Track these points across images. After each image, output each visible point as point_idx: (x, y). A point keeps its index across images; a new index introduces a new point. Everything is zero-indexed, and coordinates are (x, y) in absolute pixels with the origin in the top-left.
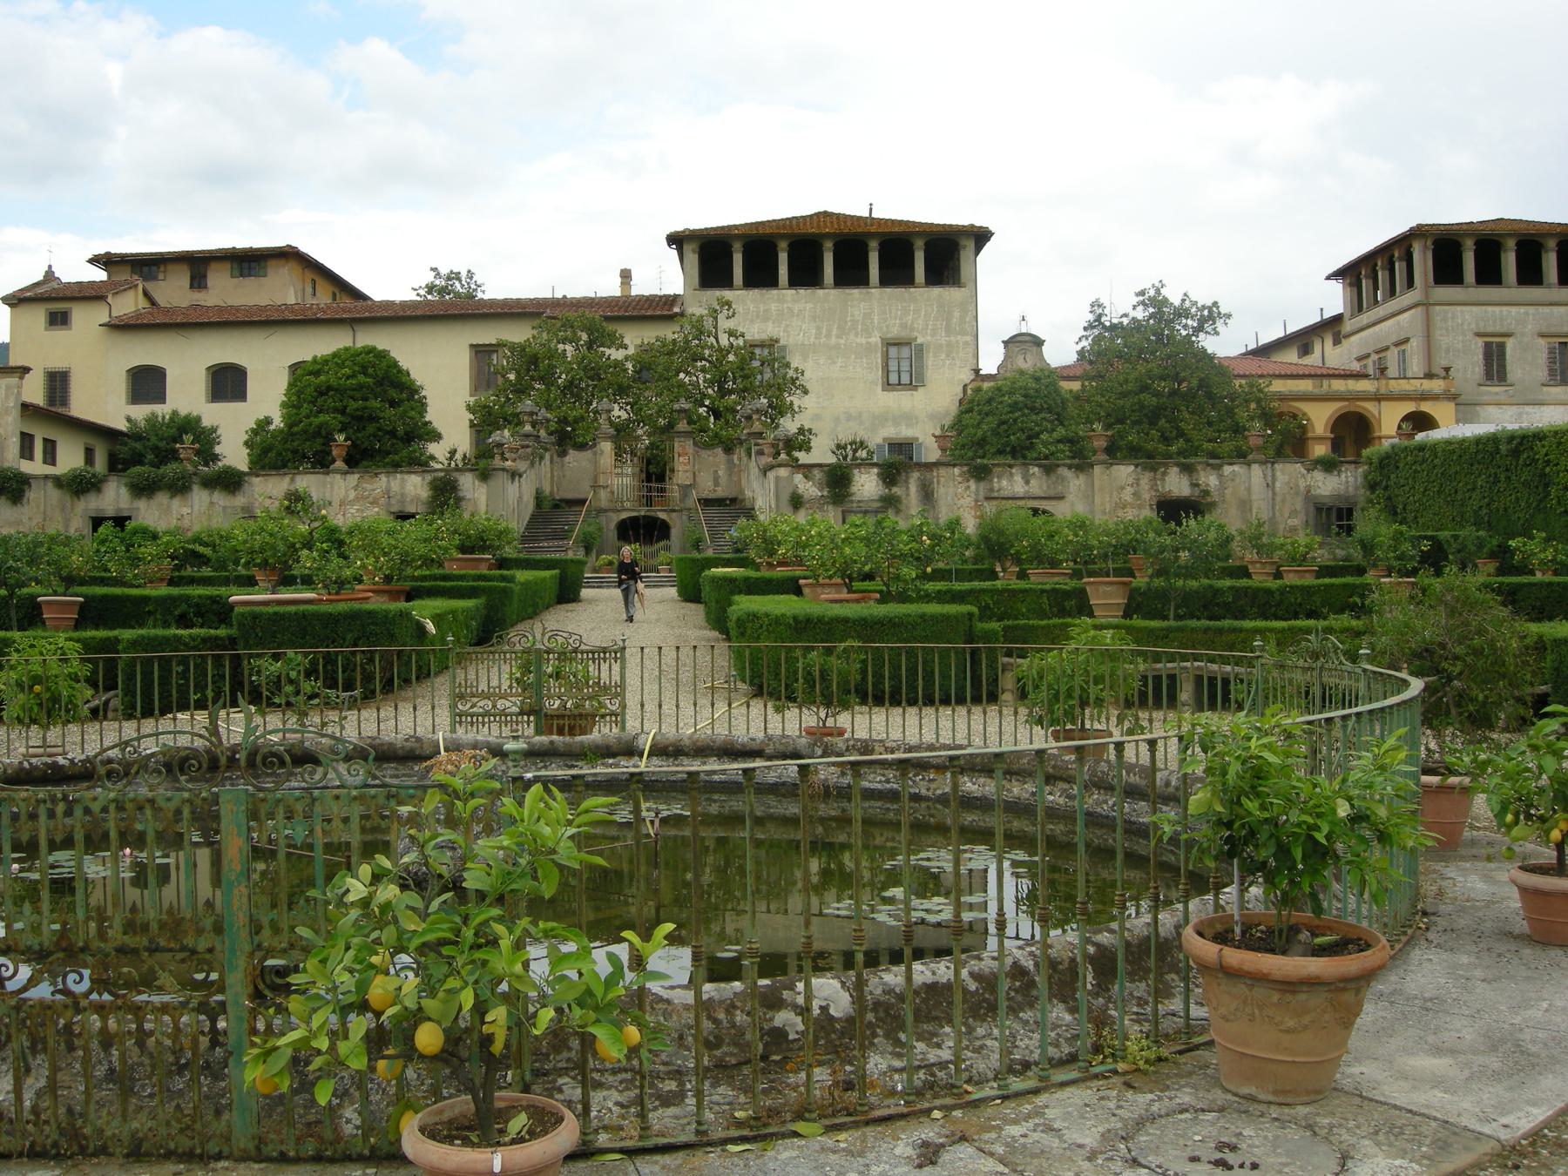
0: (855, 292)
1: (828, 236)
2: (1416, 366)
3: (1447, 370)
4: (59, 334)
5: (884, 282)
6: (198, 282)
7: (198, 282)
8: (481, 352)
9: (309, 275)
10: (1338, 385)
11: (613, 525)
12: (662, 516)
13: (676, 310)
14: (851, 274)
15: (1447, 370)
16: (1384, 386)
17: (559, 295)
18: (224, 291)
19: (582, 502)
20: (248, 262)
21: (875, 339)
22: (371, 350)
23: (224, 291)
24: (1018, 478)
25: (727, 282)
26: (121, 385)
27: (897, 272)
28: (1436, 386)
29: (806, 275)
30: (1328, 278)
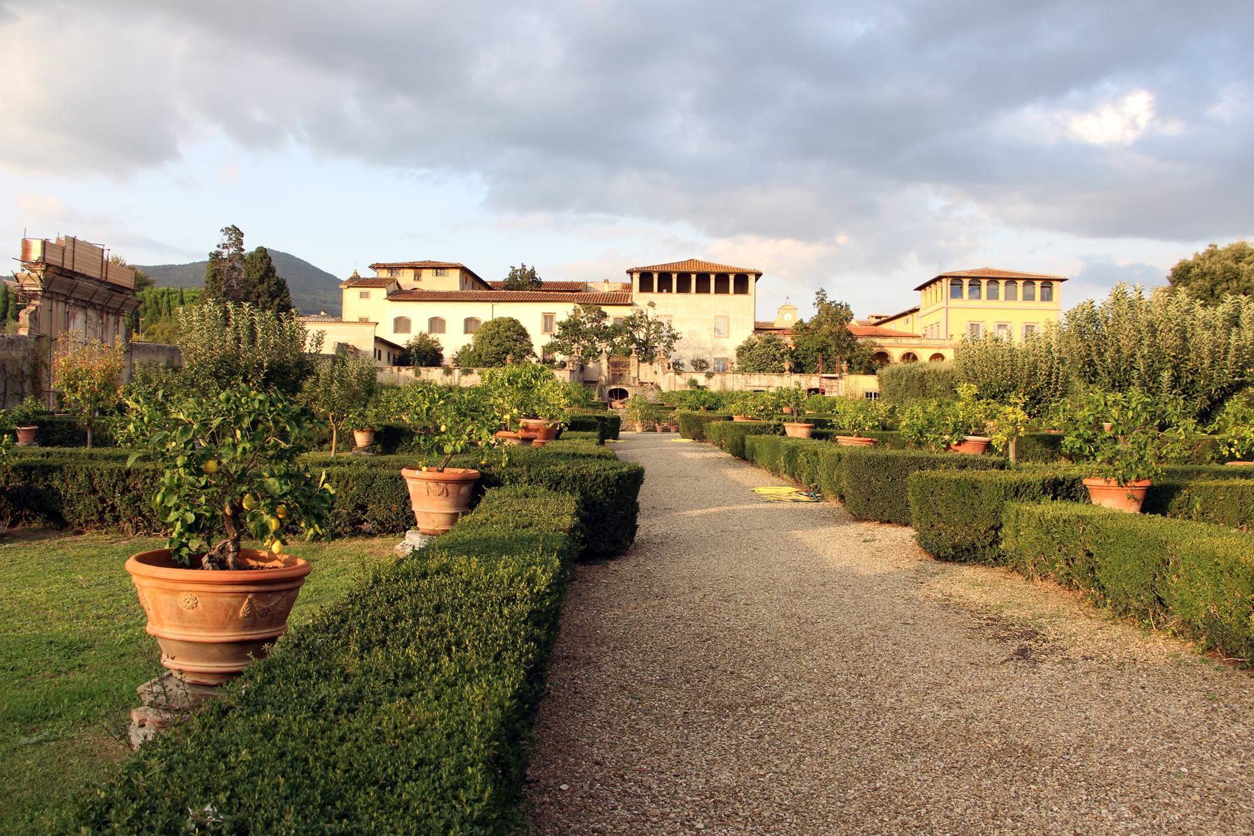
0: (703, 296)
1: (693, 273)
2: (943, 336)
3: (952, 336)
4: (365, 301)
5: (717, 292)
6: (417, 277)
7: (417, 277)
8: (548, 318)
9: (466, 275)
10: (904, 341)
11: (607, 392)
12: (626, 388)
13: (629, 302)
14: (703, 287)
15: (952, 336)
16: (924, 342)
17: (569, 281)
18: (429, 282)
19: (594, 382)
20: (439, 268)
21: (712, 316)
22: (511, 320)
23: (429, 282)
24: (757, 379)
25: (651, 290)
26: (391, 325)
27: (722, 287)
28: (947, 343)
29: (684, 287)
30: (916, 290)
